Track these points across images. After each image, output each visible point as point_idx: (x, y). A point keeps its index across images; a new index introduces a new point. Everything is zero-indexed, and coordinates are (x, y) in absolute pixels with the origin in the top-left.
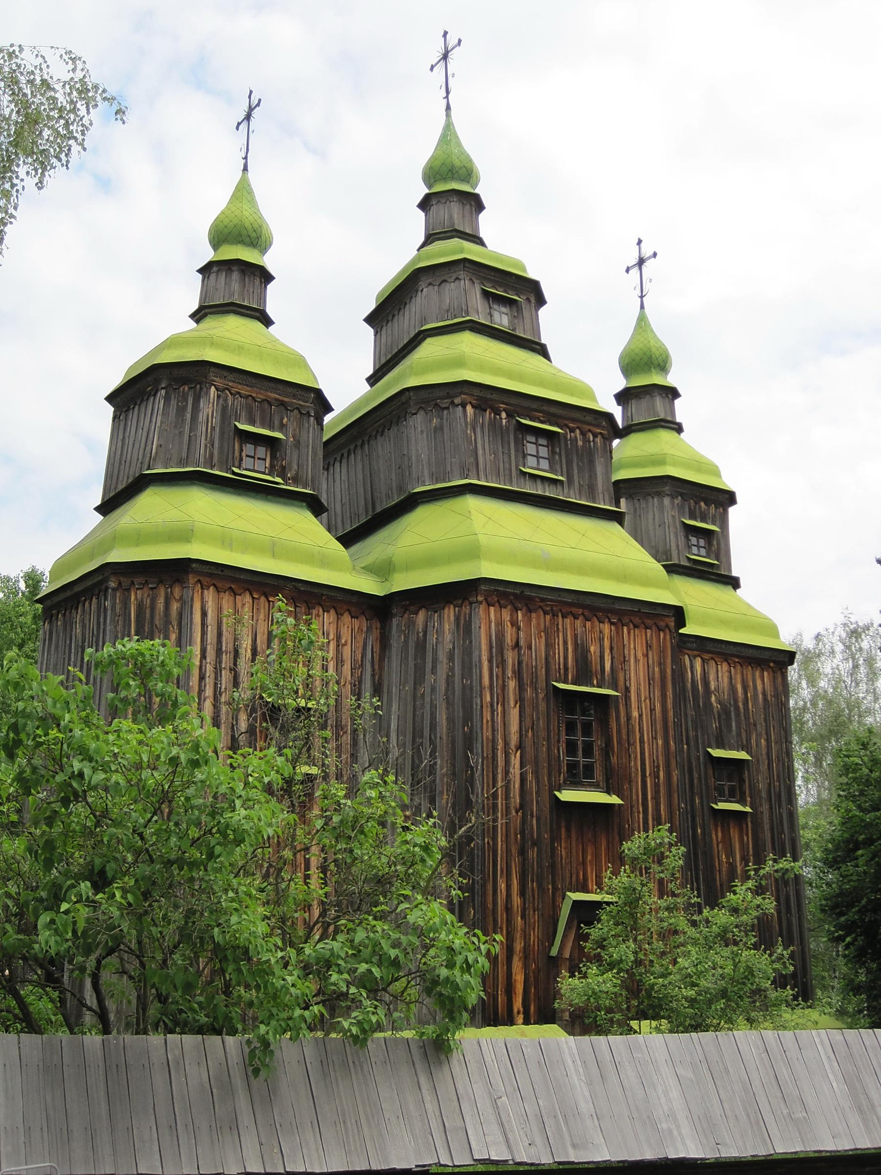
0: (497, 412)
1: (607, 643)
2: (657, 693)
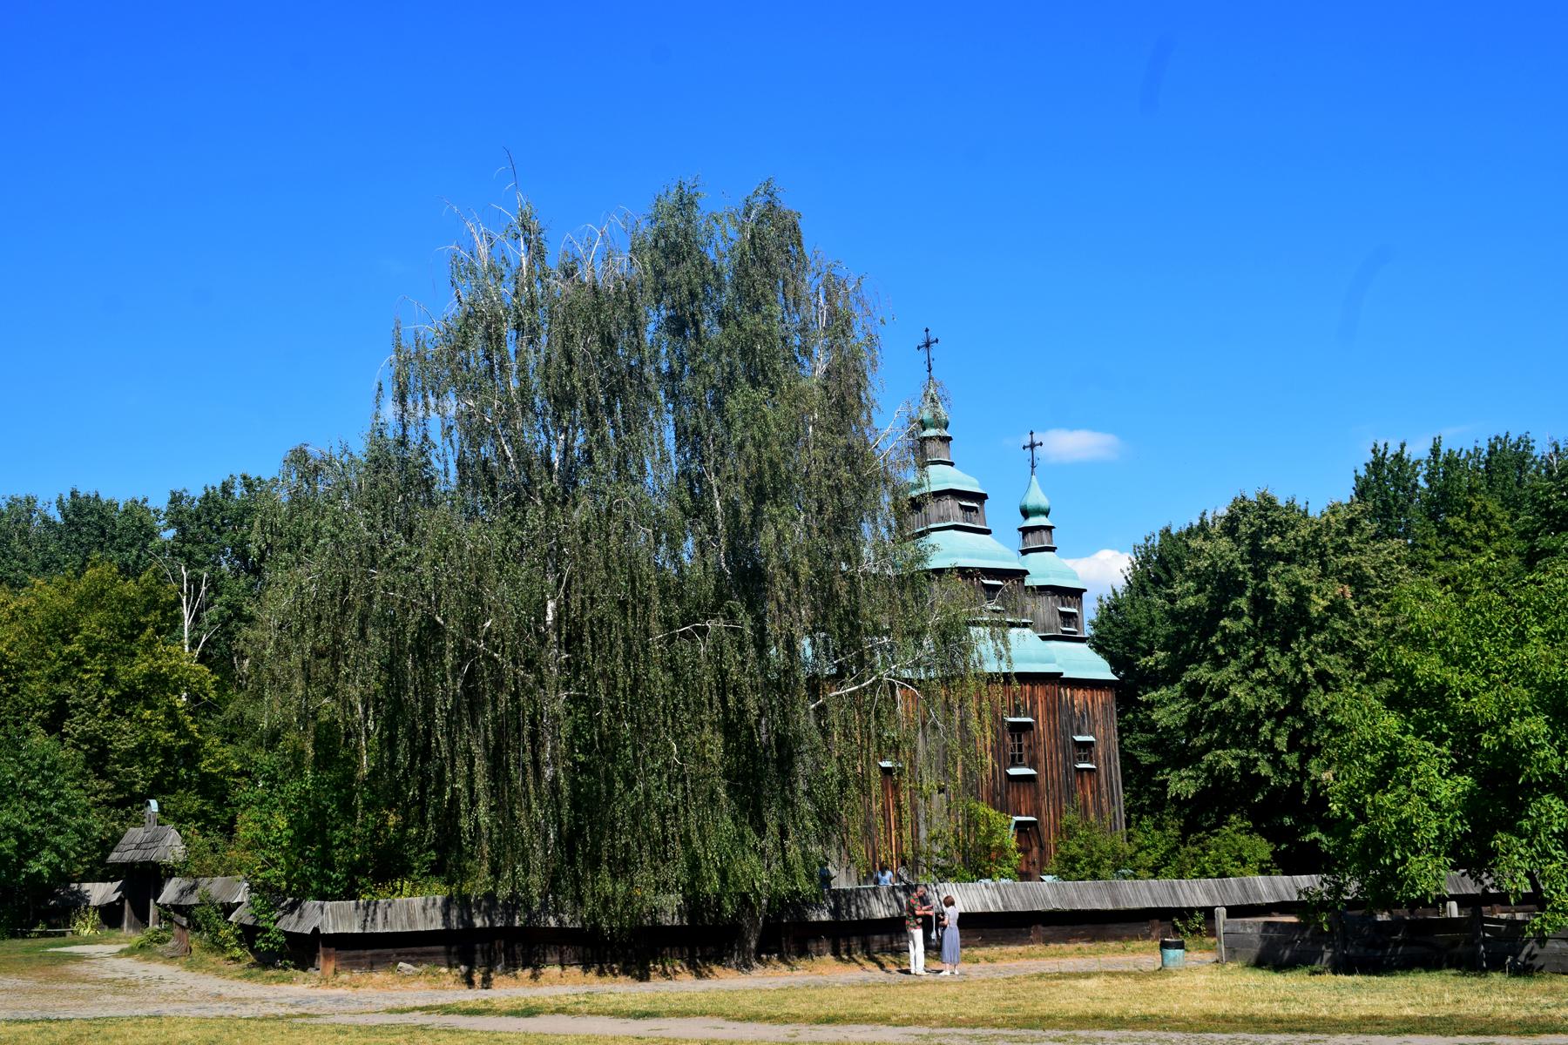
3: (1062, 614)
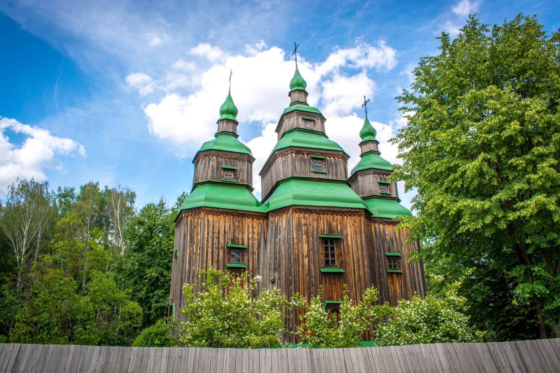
0: (303, 154)
1: (339, 221)
2: (358, 236)
3: (380, 184)
